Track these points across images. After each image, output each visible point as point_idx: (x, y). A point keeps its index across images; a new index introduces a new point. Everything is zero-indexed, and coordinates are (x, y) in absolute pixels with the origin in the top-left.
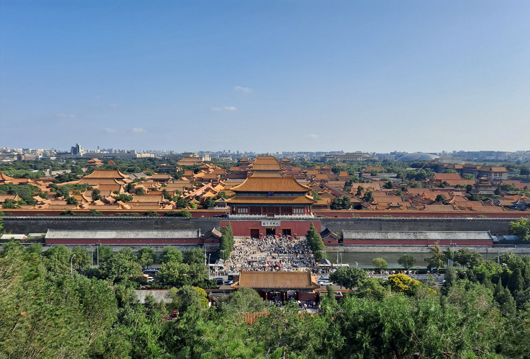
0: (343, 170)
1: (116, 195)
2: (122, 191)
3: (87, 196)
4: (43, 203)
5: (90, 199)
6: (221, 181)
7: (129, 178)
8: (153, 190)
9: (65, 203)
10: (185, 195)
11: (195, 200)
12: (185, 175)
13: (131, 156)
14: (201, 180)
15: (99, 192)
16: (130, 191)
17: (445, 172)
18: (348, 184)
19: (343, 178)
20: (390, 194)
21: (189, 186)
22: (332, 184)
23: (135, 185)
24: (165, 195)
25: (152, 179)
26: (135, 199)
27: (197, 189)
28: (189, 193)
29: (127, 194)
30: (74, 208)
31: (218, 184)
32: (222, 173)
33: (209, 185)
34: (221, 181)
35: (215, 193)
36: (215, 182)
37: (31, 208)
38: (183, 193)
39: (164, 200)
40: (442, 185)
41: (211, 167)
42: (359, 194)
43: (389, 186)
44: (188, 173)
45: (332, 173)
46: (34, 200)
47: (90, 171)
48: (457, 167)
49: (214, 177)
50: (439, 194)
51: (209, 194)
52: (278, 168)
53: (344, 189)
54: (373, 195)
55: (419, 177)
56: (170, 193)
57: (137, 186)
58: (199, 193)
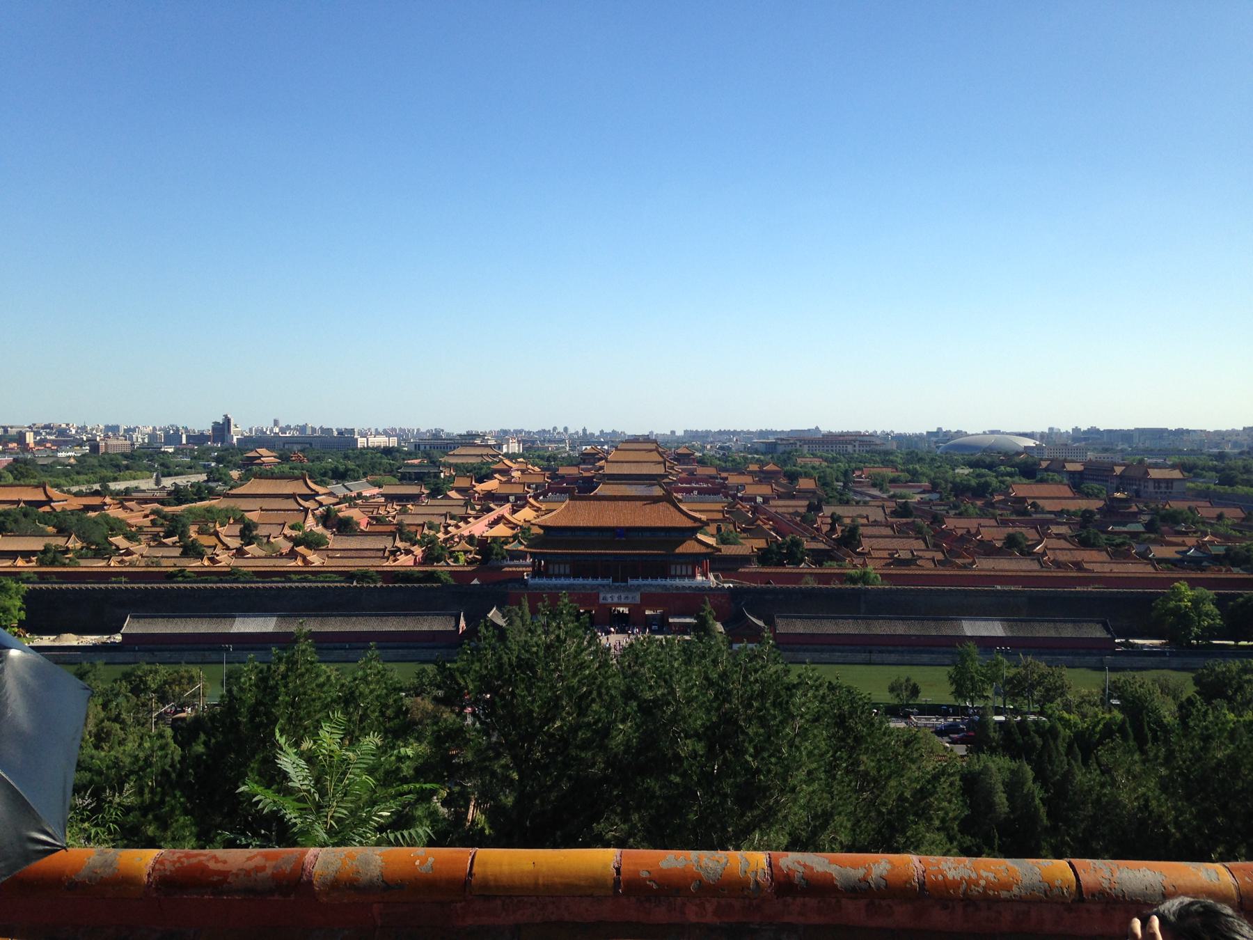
0: (807, 475)
1: (294, 533)
2: (310, 524)
3: (229, 533)
4: (129, 553)
5: (235, 543)
6: (531, 500)
7: (331, 494)
8: (379, 520)
9: (177, 552)
10: (447, 532)
11: (464, 545)
12: (456, 485)
13: (343, 442)
14: (490, 496)
15: (256, 526)
16: (329, 524)
17: (1042, 481)
18: (815, 508)
19: (803, 494)
20: (901, 532)
21: (460, 511)
22: (781, 507)
23: (340, 511)
24: (401, 534)
25: (383, 495)
26: (334, 541)
27: (476, 518)
28: (457, 527)
29: (319, 529)
30: (194, 564)
31: (523, 507)
32: (539, 480)
33: (505, 510)
34: (531, 500)
35: (513, 529)
36: (520, 502)
37: (98, 565)
38: (446, 528)
39: (399, 544)
40: (1020, 507)
41: (514, 466)
42: (833, 529)
43: (904, 510)
44: (462, 482)
45: (784, 481)
46: (111, 544)
47: (244, 479)
48: (1070, 467)
49: (519, 490)
50: (1010, 530)
51: (501, 531)
52: (660, 470)
53: (804, 518)
54: (861, 530)
55: (981, 491)
56: (413, 529)
57: (345, 512)
58: (479, 528)
